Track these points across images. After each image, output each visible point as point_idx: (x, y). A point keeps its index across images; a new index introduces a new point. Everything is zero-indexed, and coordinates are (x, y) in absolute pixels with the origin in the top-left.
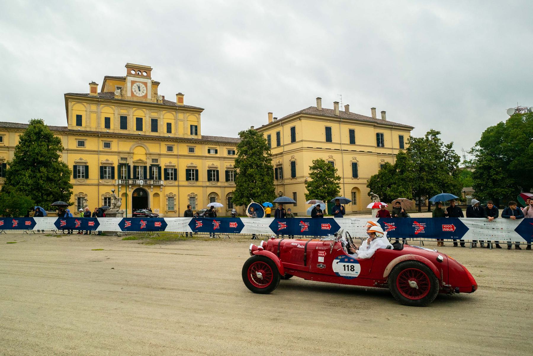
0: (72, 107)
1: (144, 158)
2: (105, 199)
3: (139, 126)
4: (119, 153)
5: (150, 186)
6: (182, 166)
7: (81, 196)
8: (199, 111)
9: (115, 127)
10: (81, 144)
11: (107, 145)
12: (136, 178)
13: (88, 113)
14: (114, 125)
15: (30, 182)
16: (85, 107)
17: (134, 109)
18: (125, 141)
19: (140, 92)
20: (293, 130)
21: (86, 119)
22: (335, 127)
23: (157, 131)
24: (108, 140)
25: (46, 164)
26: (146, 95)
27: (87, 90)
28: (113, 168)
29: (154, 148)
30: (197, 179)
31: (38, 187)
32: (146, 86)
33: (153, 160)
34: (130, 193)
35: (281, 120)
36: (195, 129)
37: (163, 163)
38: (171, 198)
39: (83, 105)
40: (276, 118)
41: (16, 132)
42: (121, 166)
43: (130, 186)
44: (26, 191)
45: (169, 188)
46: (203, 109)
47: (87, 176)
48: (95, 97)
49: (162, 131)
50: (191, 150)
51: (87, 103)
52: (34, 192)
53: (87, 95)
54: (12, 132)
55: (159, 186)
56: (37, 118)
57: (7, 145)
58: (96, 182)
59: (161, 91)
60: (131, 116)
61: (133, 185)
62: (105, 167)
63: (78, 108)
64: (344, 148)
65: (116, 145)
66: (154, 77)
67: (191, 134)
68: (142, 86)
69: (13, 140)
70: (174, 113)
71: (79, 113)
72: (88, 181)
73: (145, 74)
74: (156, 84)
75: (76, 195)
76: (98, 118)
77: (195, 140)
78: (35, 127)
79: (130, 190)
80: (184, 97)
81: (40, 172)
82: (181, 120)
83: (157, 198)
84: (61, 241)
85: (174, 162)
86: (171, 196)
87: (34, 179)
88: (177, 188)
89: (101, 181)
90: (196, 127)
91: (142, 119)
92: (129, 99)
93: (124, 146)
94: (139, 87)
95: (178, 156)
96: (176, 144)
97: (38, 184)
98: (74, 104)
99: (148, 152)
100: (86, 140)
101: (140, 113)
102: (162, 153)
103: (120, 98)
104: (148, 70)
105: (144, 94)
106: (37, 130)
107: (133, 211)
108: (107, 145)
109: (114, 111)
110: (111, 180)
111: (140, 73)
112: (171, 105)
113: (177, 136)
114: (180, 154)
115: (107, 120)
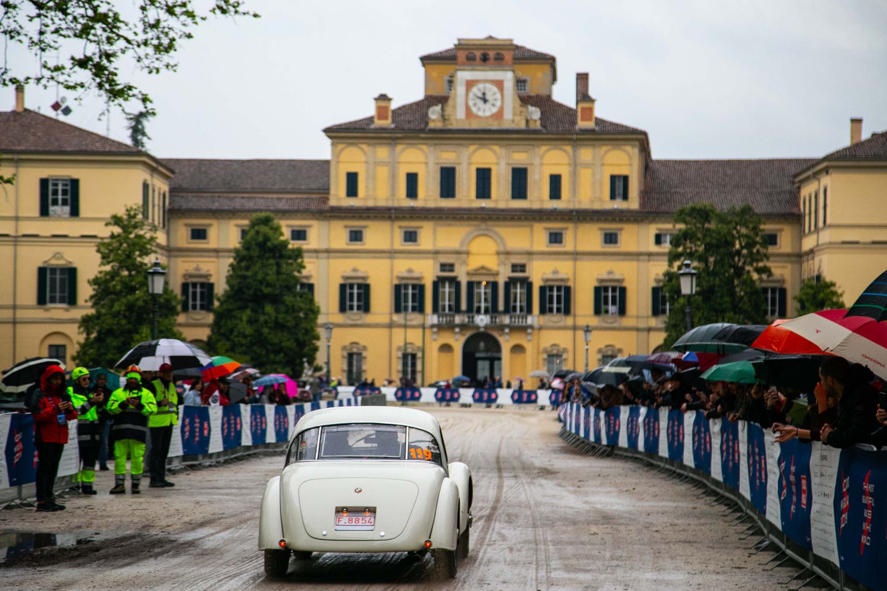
1: (492, 263)
2: (405, 356)
6: (585, 280)
9: (429, 194)
10: (356, 236)
11: (411, 236)
12: (472, 310)
17: (472, 148)
24: (411, 224)
30: (622, 311)
37: (539, 272)
42: (438, 283)
47: (365, 307)
49: (539, 196)
50: (611, 238)
51: (369, 145)
58: (385, 319)
60: (465, 166)
65: (431, 236)
71: (352, 169)
72: (369, 319)
76: (393, 176)
79: (457, 336)
86: (555, 352)
95: (576, 255)
96: (571, 226)
103: (439, 125)
108: (411, 236)
114: (580, 248)
115: (412, 180)
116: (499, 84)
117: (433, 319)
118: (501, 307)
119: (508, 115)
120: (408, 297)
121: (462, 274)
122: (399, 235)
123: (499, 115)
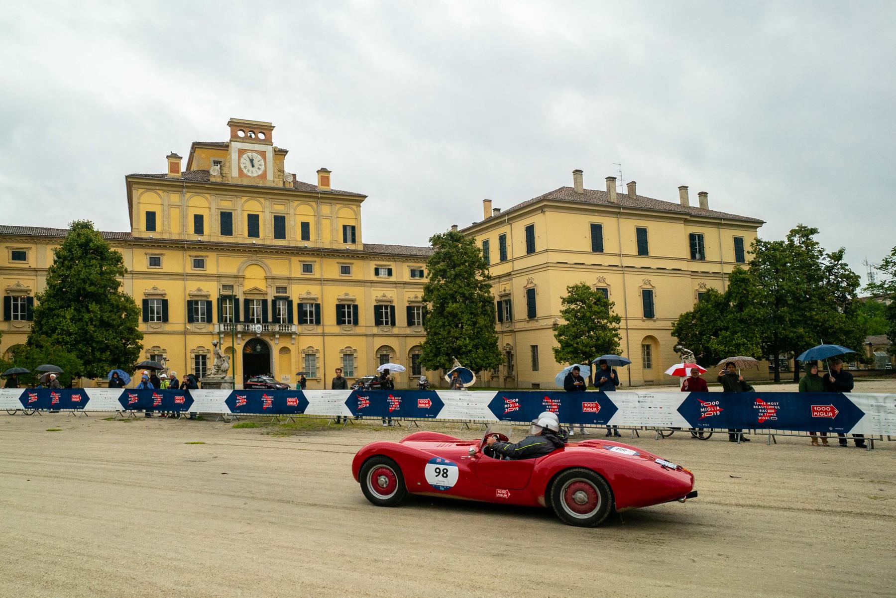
0: (139, 199)
1: (262, 285)
2: (197, 357)
3: (254, 230)
4: (220, 276)
5: (273, 334)
7: (156, 353)
8: (356, 199)
11: (199, 263)
12: (249, 320)
13: (166, 208)
14: (211, 227)
15: (73, 328)
16: (161, 198)
18: (229, 256)
19: (254, 169)
20: (530, 230)
21: (163, 217)
22: (609, 225)
23: (285, 238)
25: (98, 298)
26: (265, 173)
27: (163, 168)
28: (209, 304)
29: (280, 268)
31: (85, 338)
32: (264, 158)
33: (278, 289)
34: (239, 347)
35: (508, 213)
36: (351, 233)
38: (310, 356)
39: (157, 193)
40: (499, 210)
41: (47, 244)
43: (239, 336)
44: (66, 343)
45: (306, 339)
46: (366, 197)
48: (177, 180)
49: (294, 237)
50: (345, 270)
52: (80, 346)
53: (163, 176)
54: (41, 243)
55: (290, 335)
56: (82, 218)
57: (33, 266)
58: (181, 328)
59: (290, 166)
60: (239, 212)
61: (244, 333)
62: (196, 303)
63: (149, 201)
64: (627, 262)
65: (214, 264)
66: (278, 140)
67: (345, 241)
68: (257, 158)
69: (44, 257)
70: (314, 204)
72: (167, 327)
73: (261, 136)
74: (281, 153)
75: (147, 351)
77: (351, 252)
78: (79, 235)
80: (331, 176)
81: (88, 311)
82: (326, 217)
83: (285, 356)
84: (132, 427)
85: (314, 291)
87: (79, 324)
88: (321, 338)
89: (189, 326)
90: (353, 228)
91: (257, 216)
92: (235, 182)
94: (252, 161)
95: (322, 281)
96: (317, 260)
97: (86, 332)
98: (142, 194)
99: (269, 275)
100: (162, 255)
101: (254, 206)
102: (294, 275)
103: (219, 180)
104: (267, 129)
105: (260, 172)
106: (83, 240)
107: (245, 380)
108: (199, 263)
109: (210, 203)
110: (205, 325)
111: (253, 136)
112: (309, 189)
113: (320, 245)
115: (199, 220)
118: (270, 319)
120: (196, 310)
121: (240, 293)
122: (189, 263)
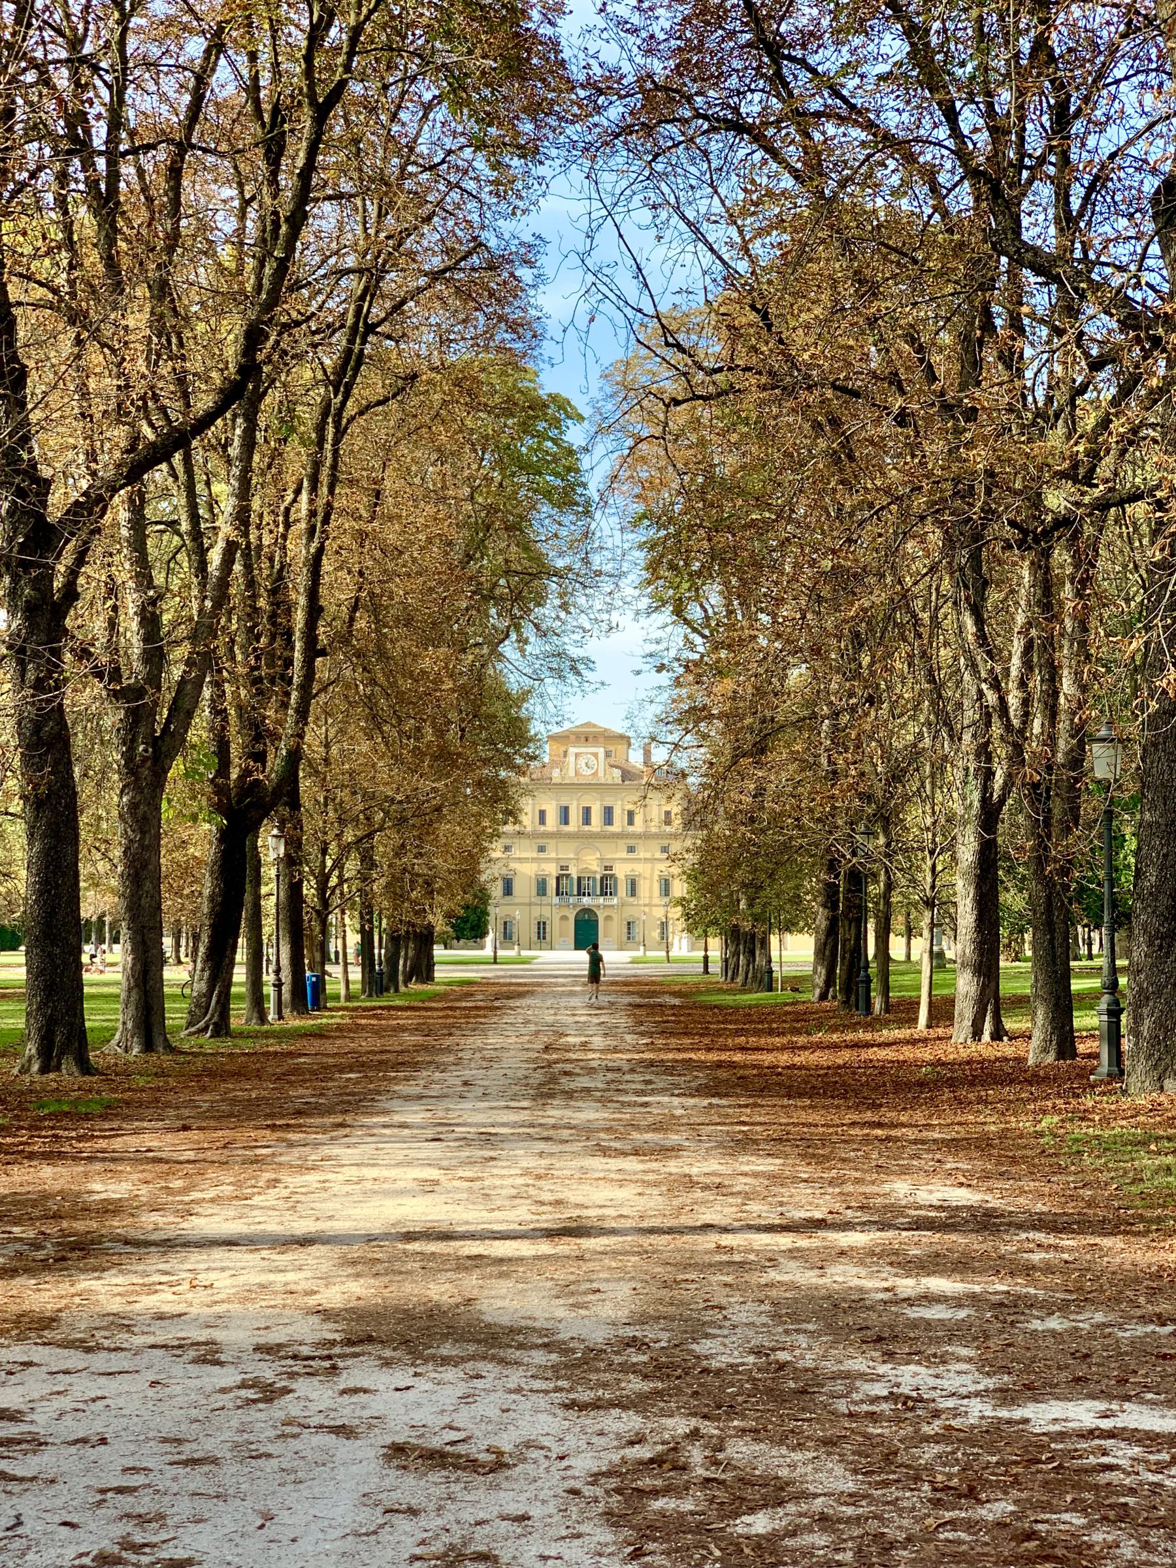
3: (587, 820)
24: (542, 842)
33: (606, 868)
85: (639, 868)
93: (566, 851)
103: (559, 781)
115: (542, 814)
116: (596, 755)
117: (556, 900)
119: (601, 774)
121: (574, 872)
122: (535, 848)
123: (595, 774)
